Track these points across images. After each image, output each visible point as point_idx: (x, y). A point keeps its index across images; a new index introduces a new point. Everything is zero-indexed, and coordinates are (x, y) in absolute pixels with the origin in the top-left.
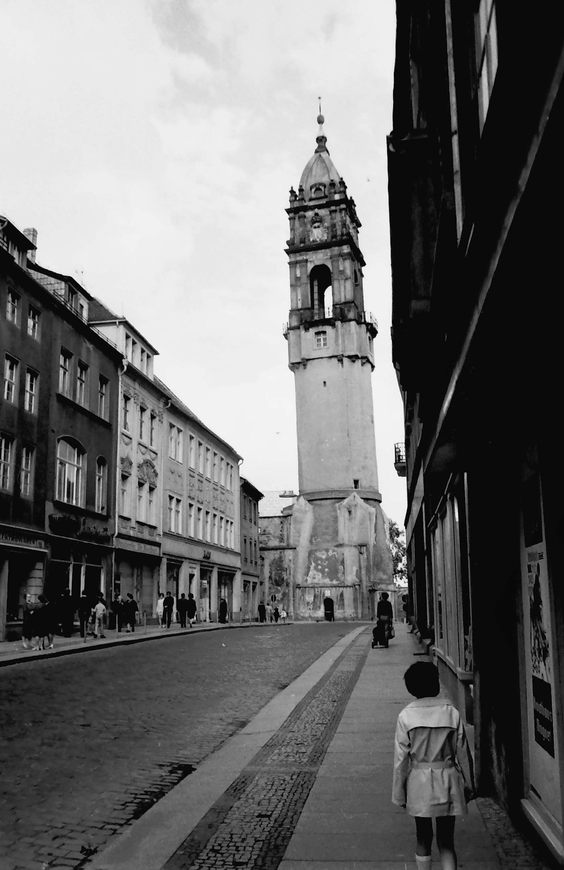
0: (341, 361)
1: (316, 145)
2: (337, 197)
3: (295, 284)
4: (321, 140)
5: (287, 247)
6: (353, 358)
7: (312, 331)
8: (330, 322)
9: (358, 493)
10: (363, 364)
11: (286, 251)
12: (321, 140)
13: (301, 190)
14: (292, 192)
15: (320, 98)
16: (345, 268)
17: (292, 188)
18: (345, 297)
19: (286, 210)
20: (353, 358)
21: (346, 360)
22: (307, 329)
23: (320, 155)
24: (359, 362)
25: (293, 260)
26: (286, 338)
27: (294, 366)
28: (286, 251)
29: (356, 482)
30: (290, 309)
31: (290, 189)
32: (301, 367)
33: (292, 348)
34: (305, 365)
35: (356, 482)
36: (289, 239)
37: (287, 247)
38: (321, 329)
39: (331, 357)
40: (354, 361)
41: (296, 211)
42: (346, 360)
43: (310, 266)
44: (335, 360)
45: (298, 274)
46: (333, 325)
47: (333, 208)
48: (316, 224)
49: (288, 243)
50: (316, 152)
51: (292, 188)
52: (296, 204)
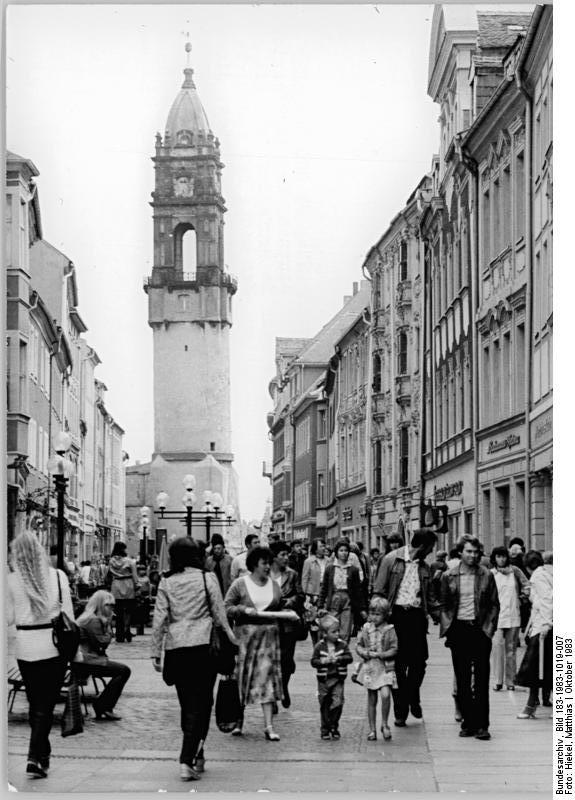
0: (203, 326)
3: (159, 239)
4: (188, 73)
5: (152, 200)
7: (176, 293)
8: (192, 286)
9: (214, 455)
10: (222, 327)
12: (188, 73)
14: (159, 138)
16: (210, 230)
17: (158, 134)
18: (209, 260)
21: (207, 325)
22: (170, 291)
23: (187, 93)
25: (158, 214)
26: (147, 292)
27: (152, 324)
29: (212, 445)
31: (156, 134)
32: (163, 327)
33: (152, 306)
35: (212, 445)
36: (153, 190)
37: (152, 200)
39: (193, 322)
41: (162, 163)
42: (207, 325)
43: (175, 223)
44: (195, 326)
45: (162, 230)
46: (197, 291)
47: (201, 163)
48: (182, 179)
49: (153, 194)
52: (162, 154)
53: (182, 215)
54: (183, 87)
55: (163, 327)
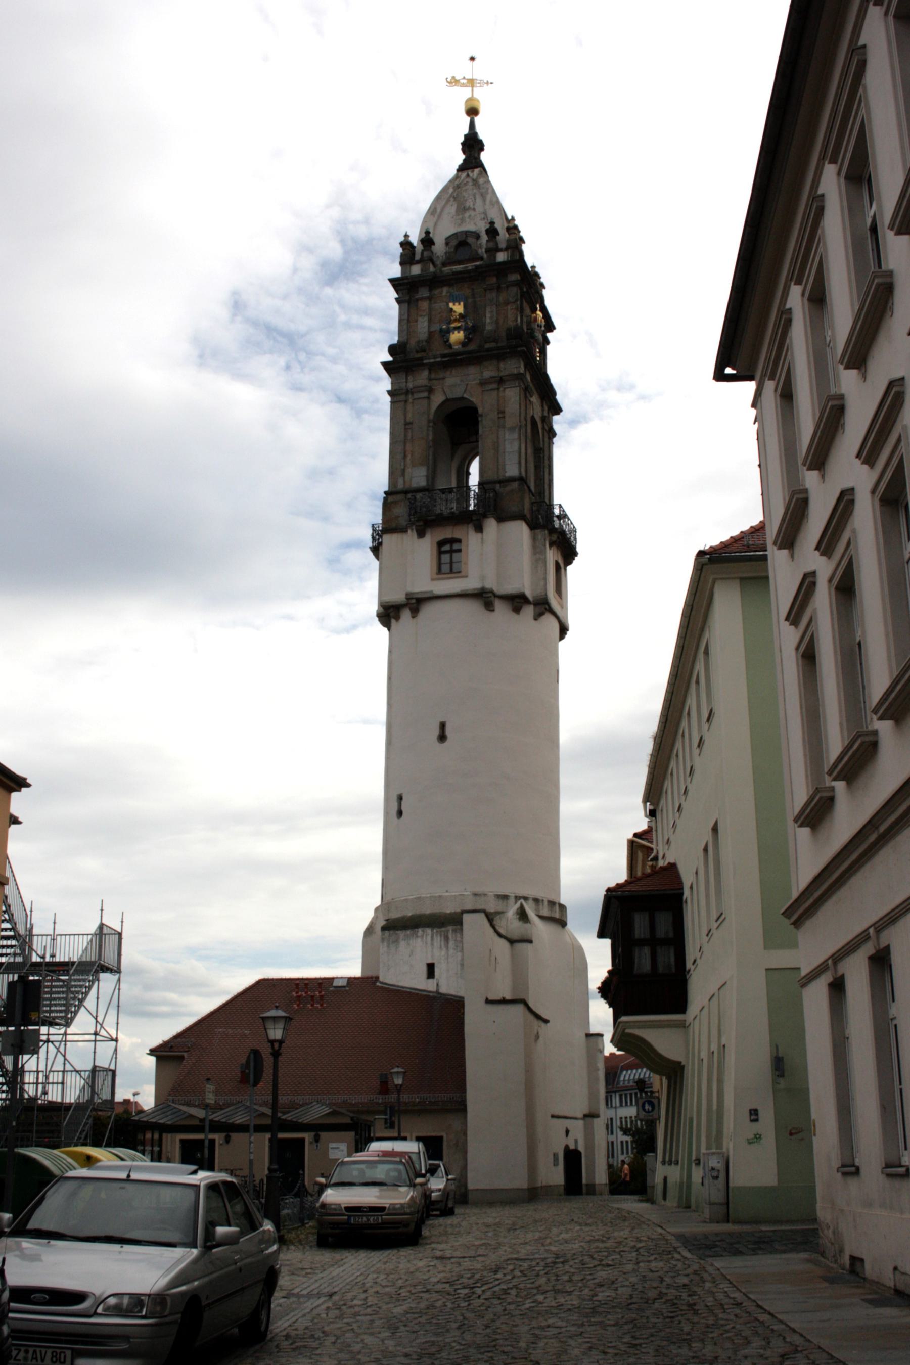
1: (460, 158)
2: (501, 257)
4: (472, 145)
5: (390, 359)
6: (517, 601)
10: (538, 616)
11: (385, 365)
12: (472, 145)
13: (427, 241)
14: (406, 244)
15: (472, 59)
17: (406, 236)
19: (392, 281)
20: (517, 601)
22: (421, 534)
24: (529, 611)
28: (385, 365)
30: (387, 489)
31: (402, 239)
34: (415, 612)
37: (390, 359)
38: (447, 533)
40: (517, 610)
46: (479, 529)
49: (392, 350)
50: (461, 169)
51: (406, 236)
52: (416, 270)
53: (458, 384)
54: (458, 170)
55: (406, 614)
